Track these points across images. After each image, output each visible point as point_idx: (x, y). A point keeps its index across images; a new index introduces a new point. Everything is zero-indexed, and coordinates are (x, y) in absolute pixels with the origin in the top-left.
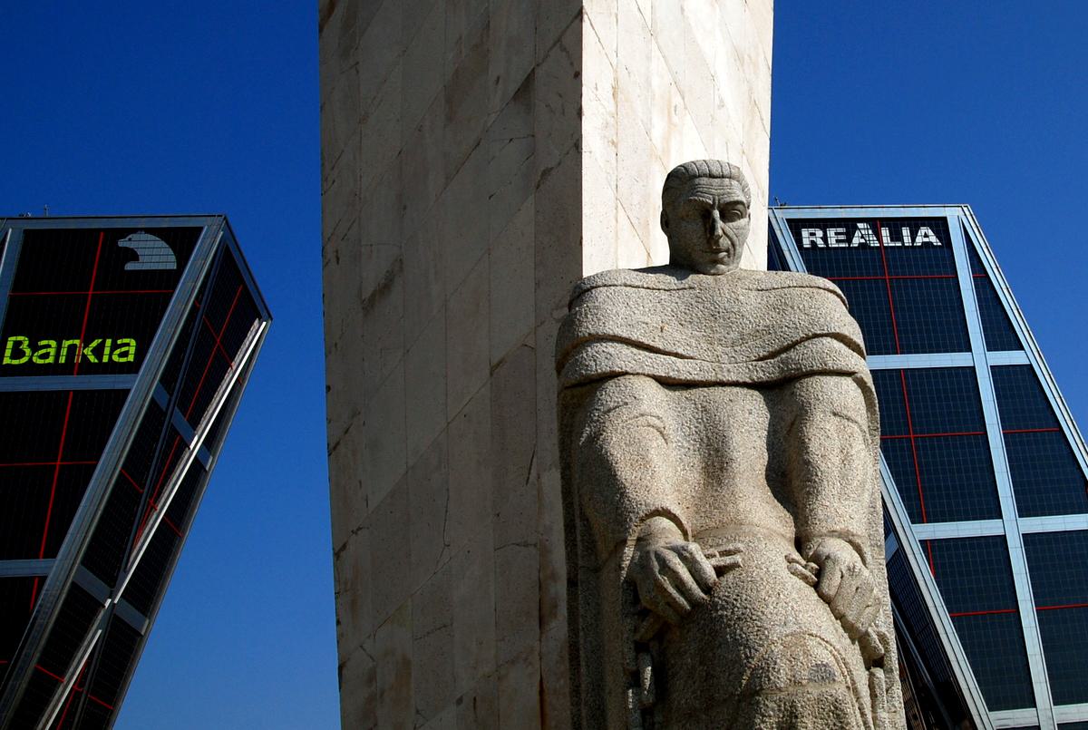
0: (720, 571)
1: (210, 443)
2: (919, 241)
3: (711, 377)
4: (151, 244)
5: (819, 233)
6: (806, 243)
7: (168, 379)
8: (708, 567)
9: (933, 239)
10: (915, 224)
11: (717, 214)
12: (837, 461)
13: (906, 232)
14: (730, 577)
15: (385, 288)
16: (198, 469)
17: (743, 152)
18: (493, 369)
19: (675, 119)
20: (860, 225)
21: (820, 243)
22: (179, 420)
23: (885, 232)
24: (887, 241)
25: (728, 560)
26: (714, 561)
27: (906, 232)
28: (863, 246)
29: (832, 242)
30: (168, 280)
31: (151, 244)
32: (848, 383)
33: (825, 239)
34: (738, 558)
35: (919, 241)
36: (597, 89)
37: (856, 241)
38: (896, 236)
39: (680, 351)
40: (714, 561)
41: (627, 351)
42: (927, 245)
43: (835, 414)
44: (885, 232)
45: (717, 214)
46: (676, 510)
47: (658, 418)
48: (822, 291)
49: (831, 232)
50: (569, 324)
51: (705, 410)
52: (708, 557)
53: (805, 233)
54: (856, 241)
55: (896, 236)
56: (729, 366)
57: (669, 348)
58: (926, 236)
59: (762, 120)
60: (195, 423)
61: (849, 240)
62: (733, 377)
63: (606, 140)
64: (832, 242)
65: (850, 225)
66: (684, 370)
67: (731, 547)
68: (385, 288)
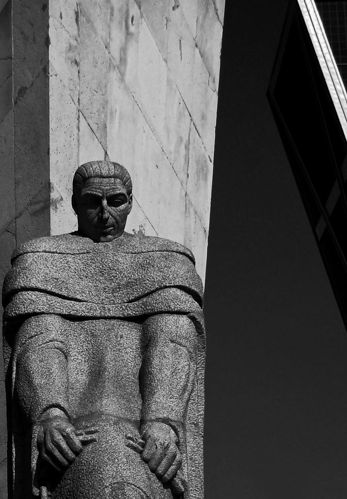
0: (85, 443)
3: (97, 313)
8: (77, 441)
11: (105, 202)
12: (169, 373)
14: (90, 447)
17: (196, 46)
19: (132, 29)
25: (89, 437)
26: (81, 438)
32: (184, 320)
34: (94, 436)
36: (61, 17)
39: (78, 297)
40: (81, 438)
41: (44, 298)
43: (172, 341)
45: (105, 202)
46: (62, 404)
47: (62, 342)
48: (175, 254)
50: (8, 279)
51: (93, 335)
52: (77, 435)
56: (109, 306)
57: (71, 295)
59: (216, 10)
62: (112, 314)
63: (70, 61)
66: (79, 309)
67: (93, 429)
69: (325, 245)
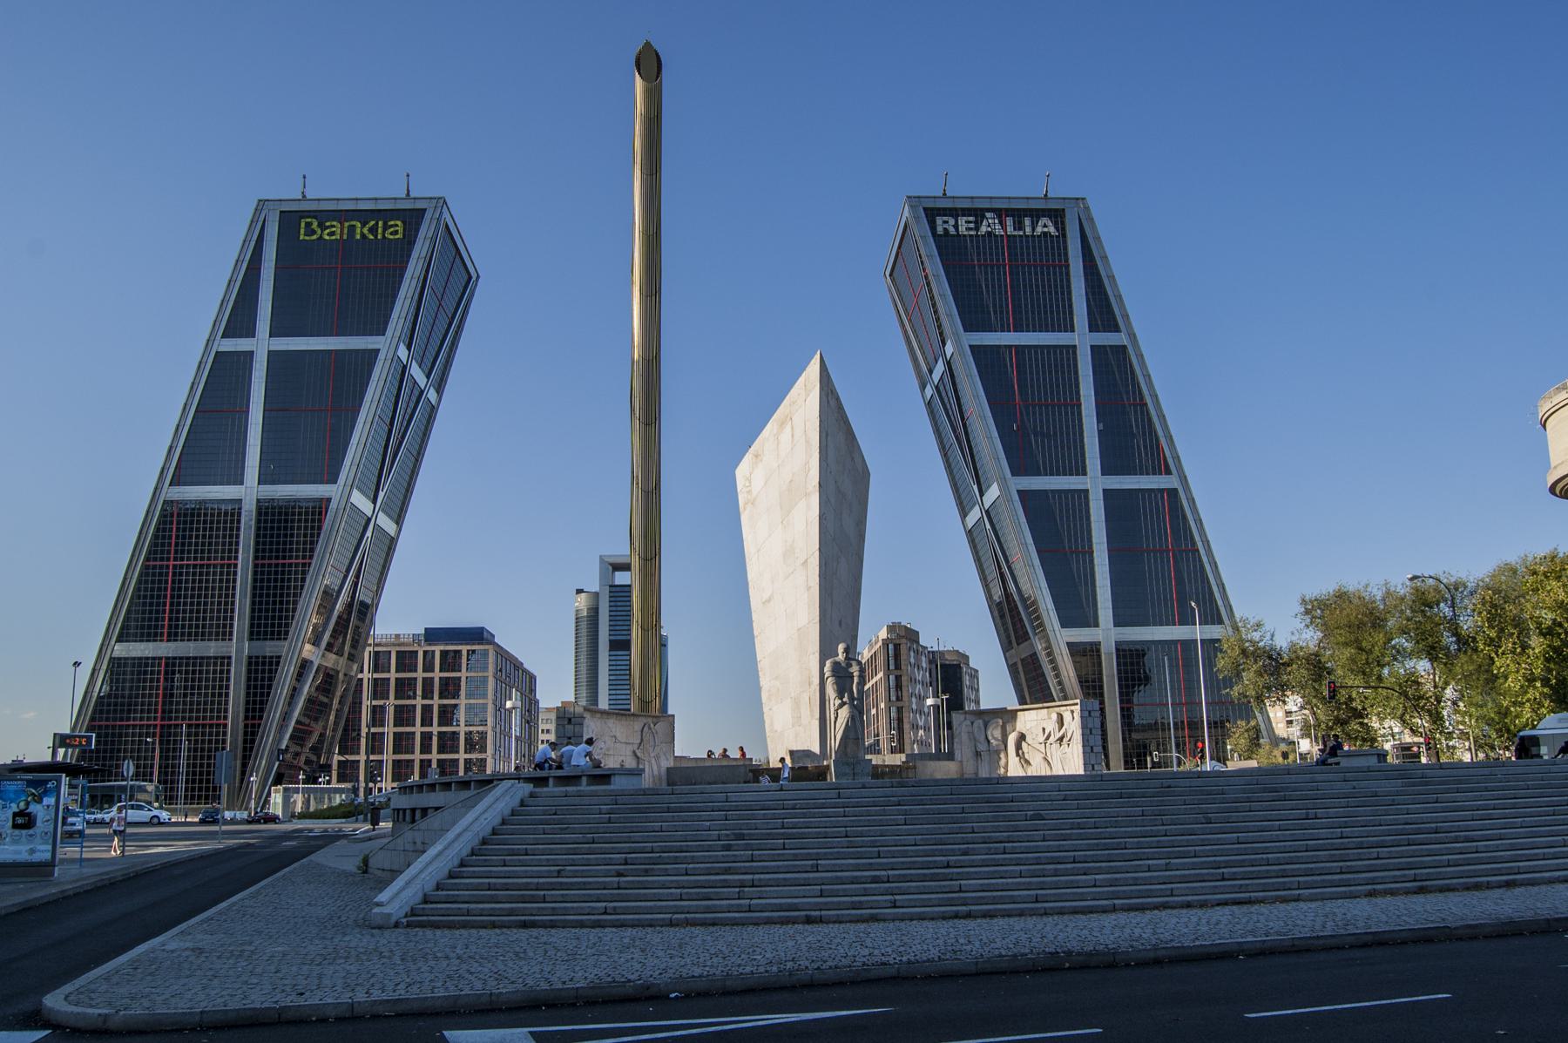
2: (1039, 230)
5: (952, 221)
6: (940, 230)
9: (1052, 229)
10: (1036, 214)
13: (1027, 221)
15: (769, 601)
20: (988, 215)
21: (952, 231)
22: (416, 372)
23: (1009, 221)
24: (1010, 230)
27: (1027, 221)
28: (989, 233)
29: (962, 229)
33: (956, 226)
35: (1039, 230)
37: (984, 229)
38: (1019, 225)
42: (1045, 234)
44: (1009, 221)
49: (962, 221)
53: (939, 220)
54: (984, 229)
55: (1019, 225)
58: (1046, 226)
61: (977, 229)
64: (962, 229)
65: (978, 214)
68: (769, 601)
69: (929, 404)
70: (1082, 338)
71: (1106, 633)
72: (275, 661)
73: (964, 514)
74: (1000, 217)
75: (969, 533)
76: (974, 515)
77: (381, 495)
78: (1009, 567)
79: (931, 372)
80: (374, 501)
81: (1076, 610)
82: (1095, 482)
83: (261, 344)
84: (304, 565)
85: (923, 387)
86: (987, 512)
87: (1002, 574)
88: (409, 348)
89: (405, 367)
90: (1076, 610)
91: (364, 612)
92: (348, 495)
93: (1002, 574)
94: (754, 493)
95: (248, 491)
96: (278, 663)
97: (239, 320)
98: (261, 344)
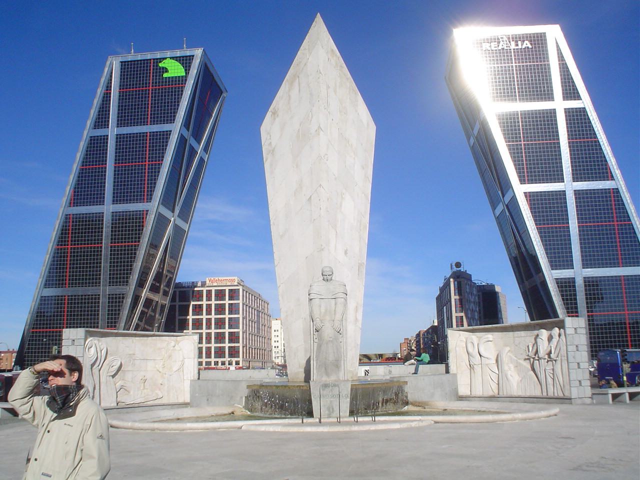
1: (206, 149)
4: (173, 64)
7: (186, 124)
16: (202, 160)
18: (306, 258)
22: (192, 141)
30: (182, 81)
31: (173, 64)
60: (199, 143)
66: (323, 297)
70: (559, 105)
71: (579, 273)
72: (121, 297)
73: (494, 208)
74: (509, 38)
75: (498, 219)
76: (500, 208)
77: (177, 210)
78: (520, 237)
79: (473, 130)
80: (173, 212)
81: (561, 259)
82: (569, 186)
83: (112, 131)
84: (135, 246)
85: (469, 139)
86: (507, 206)
87: (516, 241)
88: (188, 131)
89: (187, 140)
90: (561, 259)
91: (173, 270)
92: (153, 207)
93: (516, 241)
94: (273, 144)
95: (108, 209)
96: (123, 298)
97: (102, 120)
98: (112, 131)
